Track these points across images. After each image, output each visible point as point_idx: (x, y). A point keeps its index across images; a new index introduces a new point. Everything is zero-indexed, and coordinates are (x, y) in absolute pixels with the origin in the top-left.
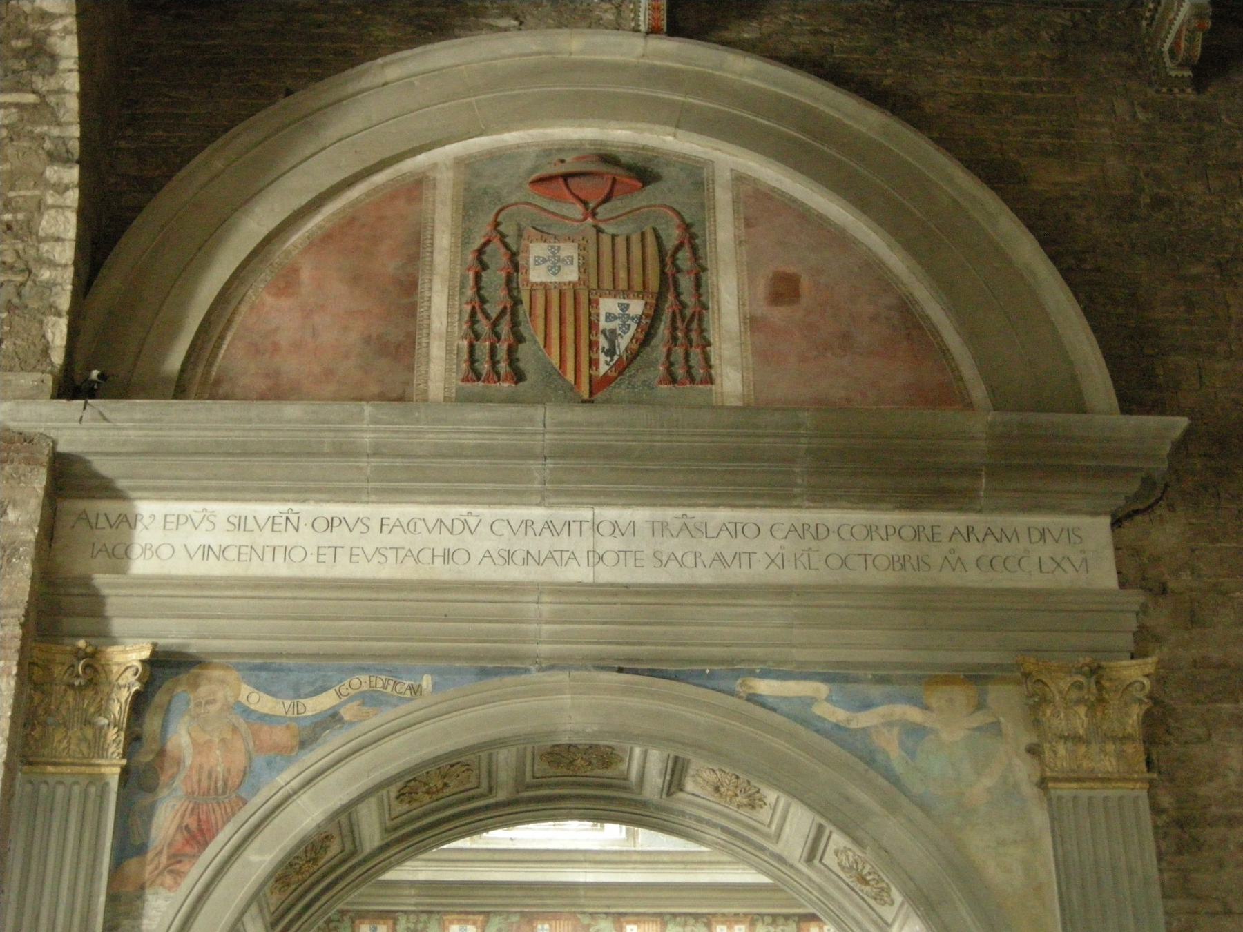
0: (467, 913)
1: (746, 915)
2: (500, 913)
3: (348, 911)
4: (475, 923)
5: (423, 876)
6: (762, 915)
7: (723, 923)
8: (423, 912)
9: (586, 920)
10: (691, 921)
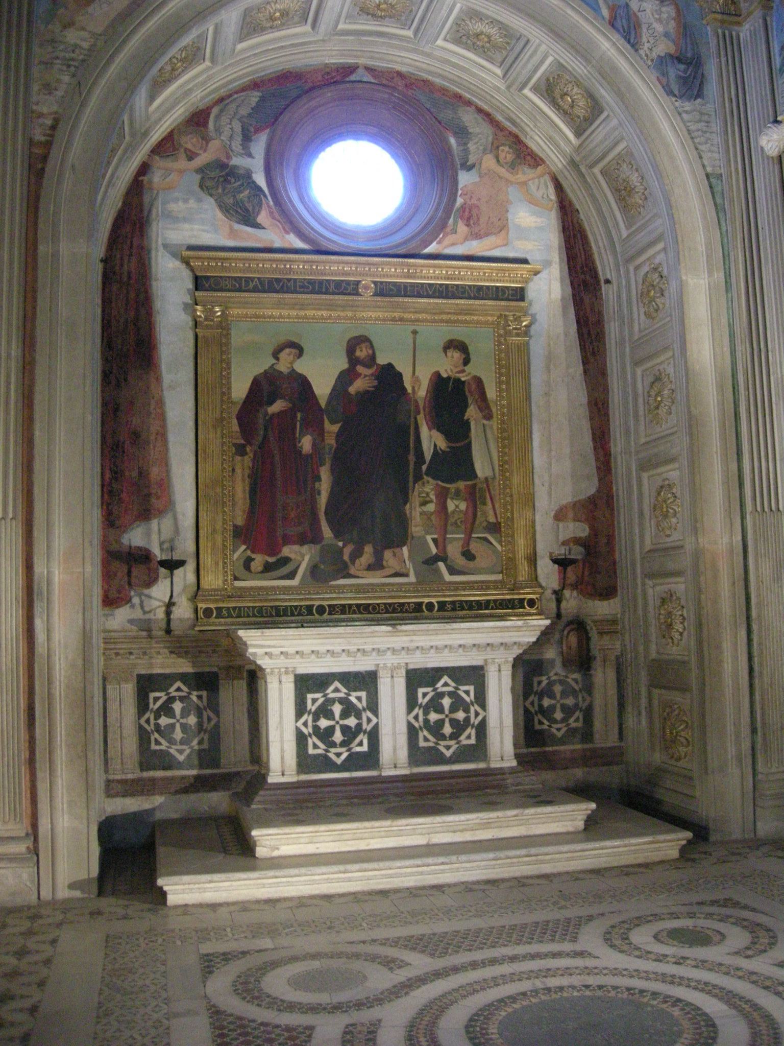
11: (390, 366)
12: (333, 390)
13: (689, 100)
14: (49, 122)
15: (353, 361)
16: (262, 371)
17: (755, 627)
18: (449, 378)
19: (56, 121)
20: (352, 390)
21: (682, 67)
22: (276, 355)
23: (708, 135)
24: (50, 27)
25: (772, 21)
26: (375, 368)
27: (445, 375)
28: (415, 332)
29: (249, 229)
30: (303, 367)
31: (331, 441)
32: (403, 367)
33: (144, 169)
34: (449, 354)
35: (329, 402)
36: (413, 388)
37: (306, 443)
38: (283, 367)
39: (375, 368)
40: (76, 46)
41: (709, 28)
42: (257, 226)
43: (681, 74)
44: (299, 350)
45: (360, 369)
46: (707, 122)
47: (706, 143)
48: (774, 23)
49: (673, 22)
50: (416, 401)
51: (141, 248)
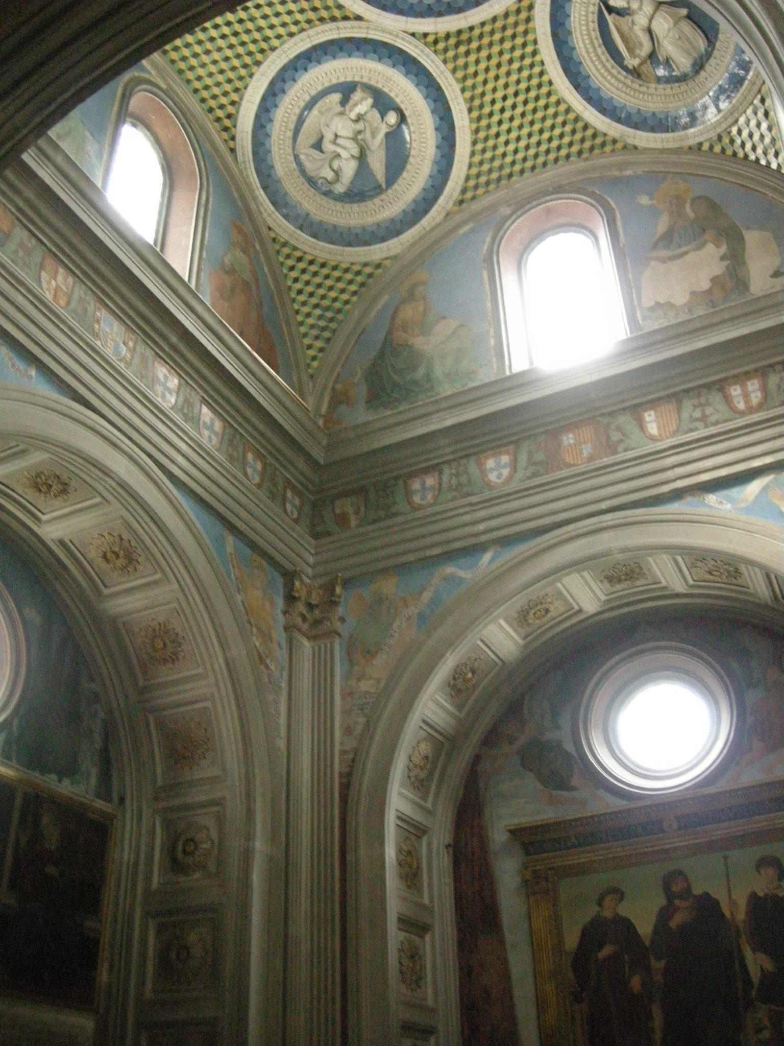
0: (499, 446)
1: (756, 370)
2: (528, 437)
3: (401, 476)
4: (507, 453)
5: (449, 423)
6: (771, 366)
7: (735, 384)
8: (461, 458)
9: (605, 420)
10: (705, 391)
11: (707, 896)
12: (655, 927)
14: (351, 756)
15: (670, 896)
16: (588, 919)
18: (766, 895)
19: (355, 754)
20: (673, 924)
22: (600, 903)
24: (350, 683)
26: (691, 900)
27: (761, 894)
28: (725, 858)
29: (565, 793)
30: (624, 910)
31: (659, 978)
32: (720, 895)
33: (477, 759)
34: (763, 872)
35: (652, 942)
36: (732, 913)
37: (636, 983)
38: (607, 914)
39: (691, 900)
40: (366, 692)
42: (571, 789)
44: (618, 894)
45: (677, 902)
50: (737, 927)
51: (481, 828)
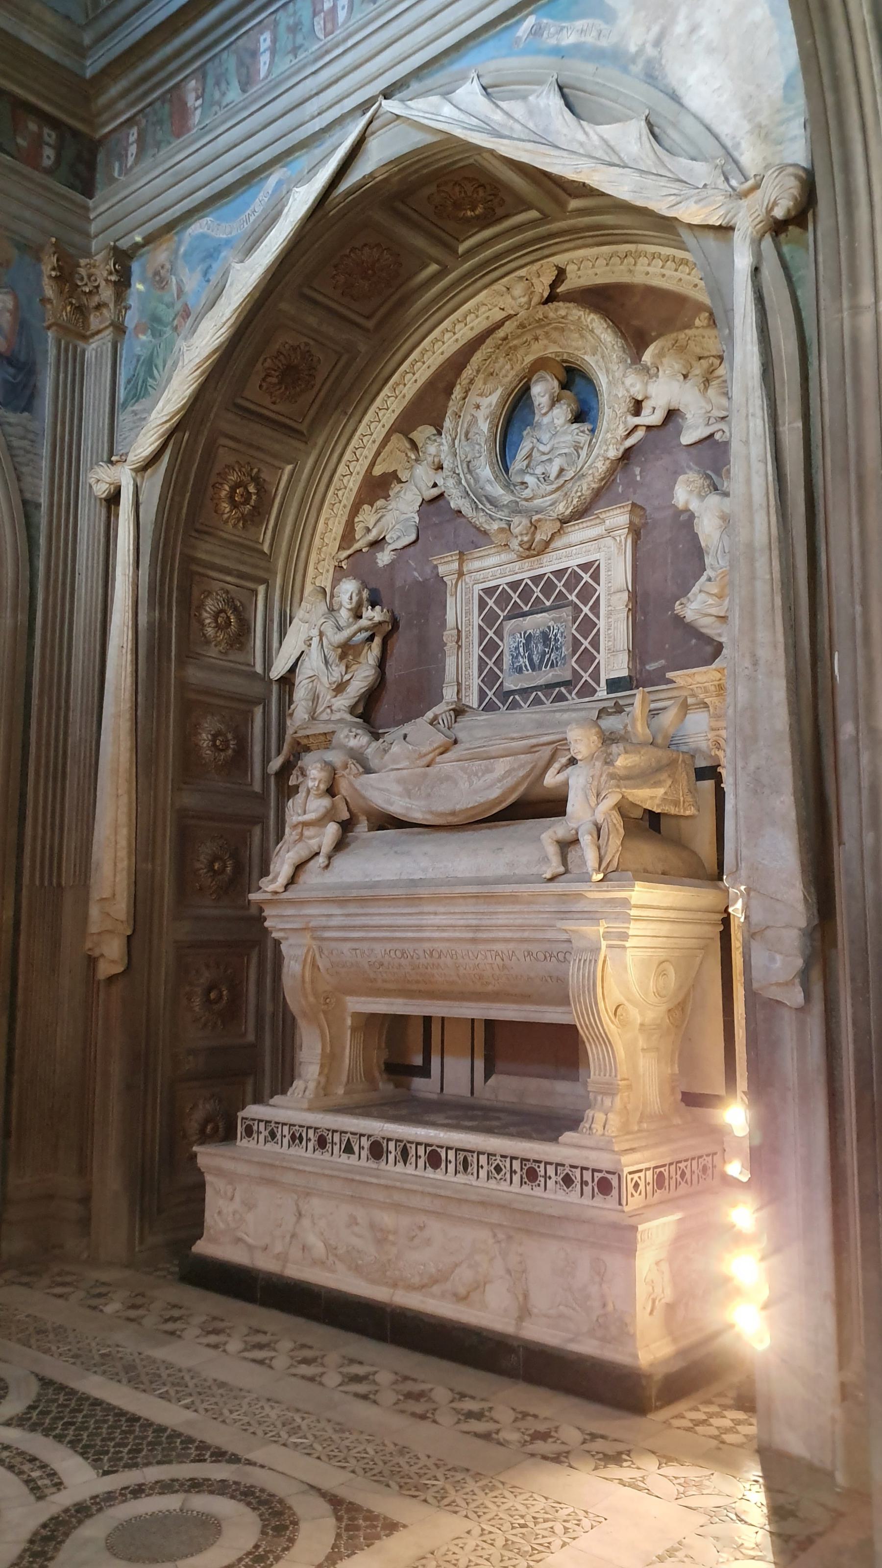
13: (15, 410)
17: (19, 1015)
21: (12, 371)
23: (31, 456)
25: (122, 349)
41: (50, 333)
43: (11, 379)
46: (32, 441)
47: (28, 465)
48: (124, 352)
49: (8, 314)
